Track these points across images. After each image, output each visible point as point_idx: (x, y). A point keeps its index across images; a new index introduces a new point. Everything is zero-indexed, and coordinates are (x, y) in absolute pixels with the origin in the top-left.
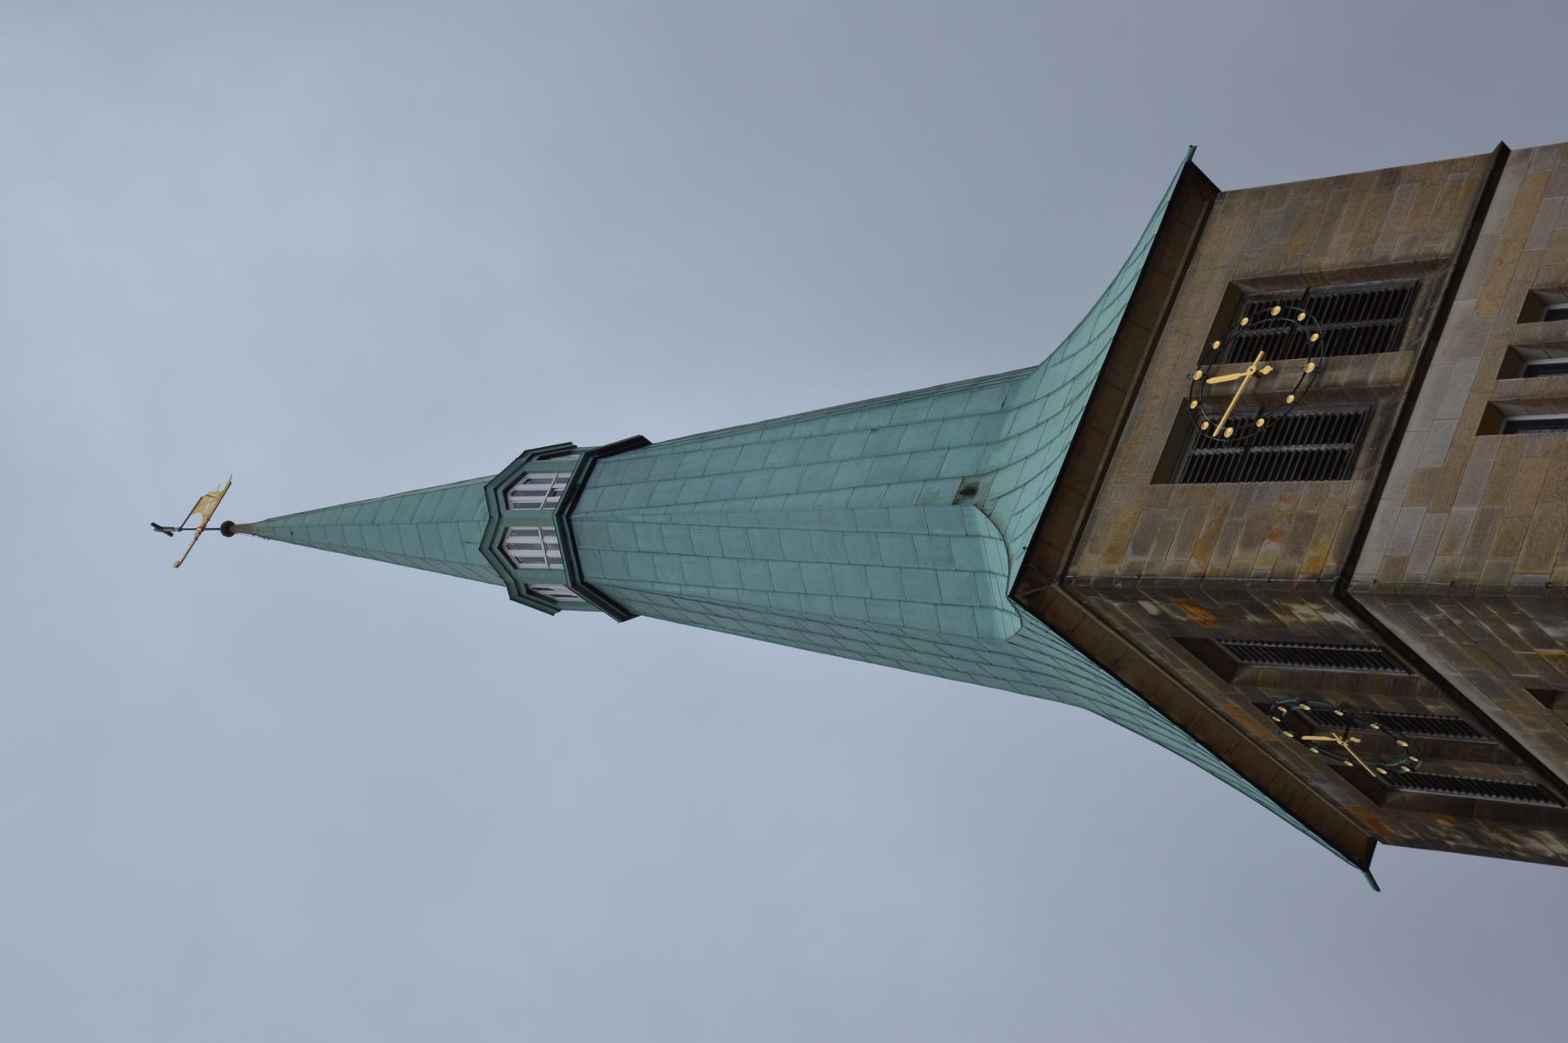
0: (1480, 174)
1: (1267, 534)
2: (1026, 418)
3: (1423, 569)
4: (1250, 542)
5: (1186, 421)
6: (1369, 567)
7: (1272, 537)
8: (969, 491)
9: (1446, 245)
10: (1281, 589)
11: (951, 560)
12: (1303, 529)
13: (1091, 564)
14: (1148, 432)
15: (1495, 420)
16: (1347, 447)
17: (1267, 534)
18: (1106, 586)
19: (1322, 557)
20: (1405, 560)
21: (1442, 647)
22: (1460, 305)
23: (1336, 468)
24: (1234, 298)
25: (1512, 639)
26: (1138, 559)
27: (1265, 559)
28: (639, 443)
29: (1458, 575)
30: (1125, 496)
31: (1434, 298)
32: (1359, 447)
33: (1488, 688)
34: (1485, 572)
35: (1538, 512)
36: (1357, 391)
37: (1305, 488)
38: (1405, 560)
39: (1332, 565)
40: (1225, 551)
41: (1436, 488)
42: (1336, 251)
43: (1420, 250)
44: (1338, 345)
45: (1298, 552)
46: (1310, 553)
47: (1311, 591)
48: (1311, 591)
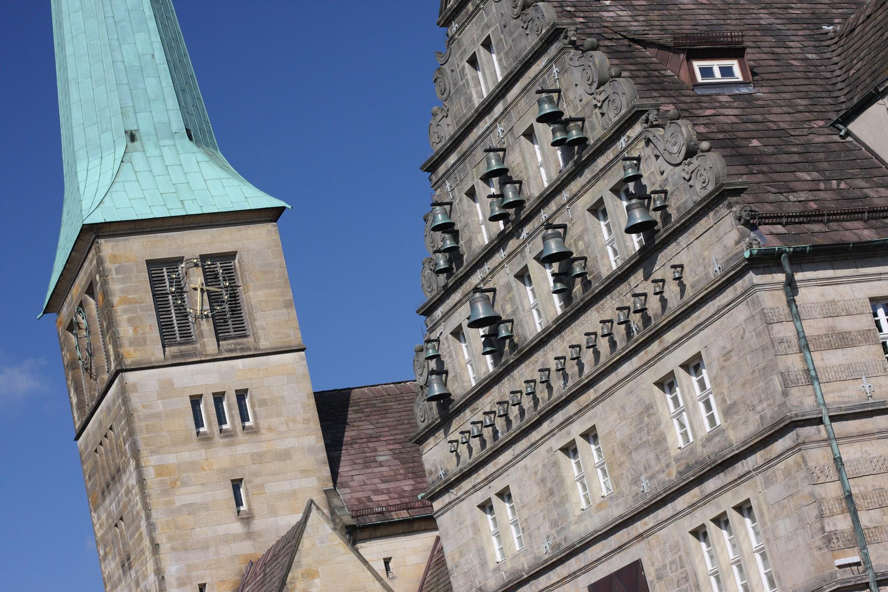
2: (168, 153)
3: (135, 400)
4: (130, 321)
5: (173, 263)
6: (130, 377)
7: (135, 329)
8: (132, 137)
9: (265, 344)
10: (117, 344)
11: (103, 132)
15: (195, 401)
16: (178, 339)
18: (100, 261)
19: (131, 355)
20: (137, 391)
26: (114, 272)
27: (125, 331)
29: (135, 415)
31: (242, 349)
32: (180, 344)
33: (109, 409)
34: (139, 424)
35: (164, 434)
36: (201, 334)
38: (137, 391)
40: (125, 311)
41: (167, 390)
43: (261, 333)
45: (131, 344)
46: (131, 350)
47: (119, 357)
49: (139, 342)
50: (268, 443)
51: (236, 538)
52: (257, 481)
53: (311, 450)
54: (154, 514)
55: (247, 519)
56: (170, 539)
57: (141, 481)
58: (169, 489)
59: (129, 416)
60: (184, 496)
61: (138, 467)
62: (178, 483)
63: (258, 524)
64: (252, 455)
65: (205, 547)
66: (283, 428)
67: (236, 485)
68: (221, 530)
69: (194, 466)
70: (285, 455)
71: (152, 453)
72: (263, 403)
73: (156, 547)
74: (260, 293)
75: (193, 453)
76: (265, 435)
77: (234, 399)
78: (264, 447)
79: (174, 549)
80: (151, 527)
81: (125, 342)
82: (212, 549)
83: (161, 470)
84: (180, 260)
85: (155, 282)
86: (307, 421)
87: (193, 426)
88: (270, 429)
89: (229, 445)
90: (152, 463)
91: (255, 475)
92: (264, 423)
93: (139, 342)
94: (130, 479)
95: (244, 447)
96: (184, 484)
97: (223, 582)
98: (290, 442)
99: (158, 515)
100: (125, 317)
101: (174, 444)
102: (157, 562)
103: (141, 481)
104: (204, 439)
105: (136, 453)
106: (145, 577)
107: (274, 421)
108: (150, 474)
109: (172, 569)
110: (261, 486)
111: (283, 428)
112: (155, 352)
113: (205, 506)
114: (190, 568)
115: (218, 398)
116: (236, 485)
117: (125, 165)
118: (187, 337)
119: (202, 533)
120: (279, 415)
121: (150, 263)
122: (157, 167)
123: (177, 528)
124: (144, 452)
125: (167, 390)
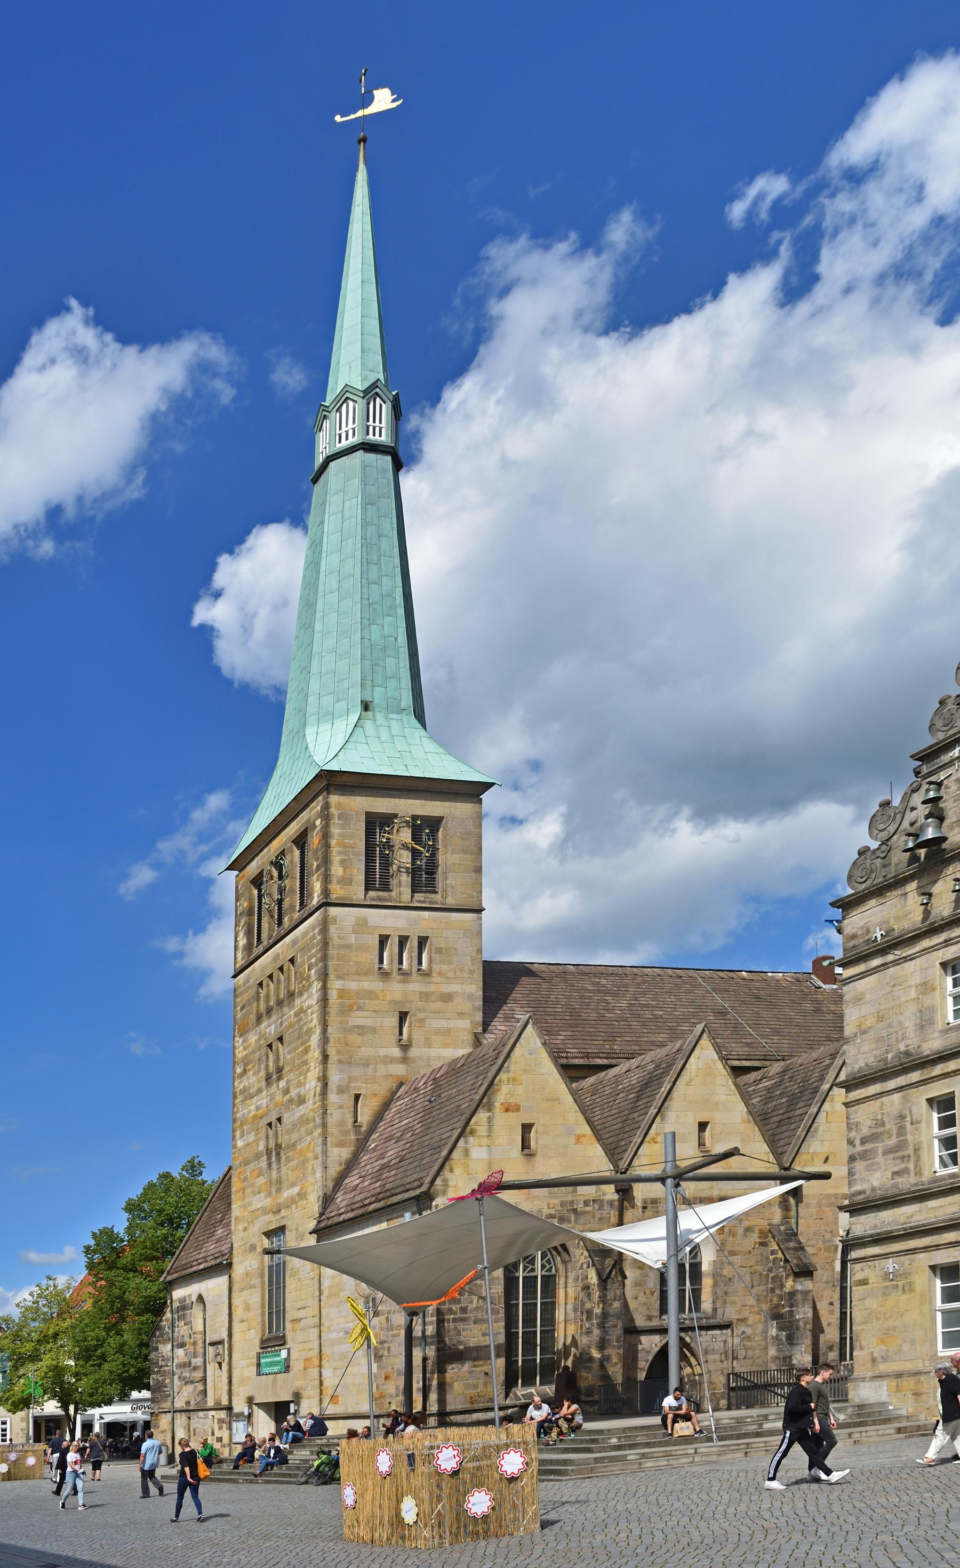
1: (347, 866)
3: (332, 929)
4: (342, 862)
6: (333, 911)
7: (344, 870)
9: (451, 901)
10: (326, 879)
14: (382, 805)
18: (326, 806)
20: (336, 923)
22: (426, 914)
23: (369, 886)
27: (337, 870)
30: (361, 804)
31: (430, 902)
34: (332, 952)
36: (400, 884)
38: (336, 923)
39: (334, 897)
40: (340, 853)
41: (361, 925)
44: (414, 872)
45: (339, 882)
46: (339, 887)
48: (326, 892)
49: (346, 881)
50: (437, 986)
51: (393, 1060)
52: (421, 1015)
53: (471, 997)
54: (330, 1030)
55: (405, 1047)
56: (339, 1052)
57: (324, 1000)
58: (345, 1011)
59: (325, 944)
60: (358, 1019)
61: (324, 989)
62: (355, 1007)
63: (413, 1052)
64: (421, 993)
65: (366, 1065)
66: (451, 975)
67: (403, 1016)
68: (382, 1052)
69: (371, 995)
70: (447, 998)
71: (338, 978)
72: (439, 951)
73: (325, 1057)
74: (455, 856)
75: (372, 984)
76: (436, 978)
77: (416, 944)
78: (432, 988)
79: (340, 1061)
81: (334, 880)
82: (372, 1067)
83: (342, 993)
84: (396, 816)
85: (370, 833)
86: (472, 972)
87: (377, 961)
88: (440, 974)
89: (404, 982)
90: (337, 987)
91: (420, 1010)
92: (436, 968)
93: (346, 881)
95: (416, 986)
96: (360, 1009)
97: (375, 1095)
98: (455, 988)
100: (339, 858)
101: (358, 974)
102: (325, 1070)
104: (384, 975)
105: (324, 977)
107: (445, 968)
108: (333, 995)
109: (335, 1078)
110: (422, 1021)
111: (451, 975)
112: (358, 892)
113: (373, 1030)
114: (350, 1079)
115: (403, 941)
116: (403, 1016)
117: (359, 730)
118: (386, 887)
119: (366, 1052)
120: (450, 963)
123: (346, 1044)
124: (332, 976)
125: (361, 925)
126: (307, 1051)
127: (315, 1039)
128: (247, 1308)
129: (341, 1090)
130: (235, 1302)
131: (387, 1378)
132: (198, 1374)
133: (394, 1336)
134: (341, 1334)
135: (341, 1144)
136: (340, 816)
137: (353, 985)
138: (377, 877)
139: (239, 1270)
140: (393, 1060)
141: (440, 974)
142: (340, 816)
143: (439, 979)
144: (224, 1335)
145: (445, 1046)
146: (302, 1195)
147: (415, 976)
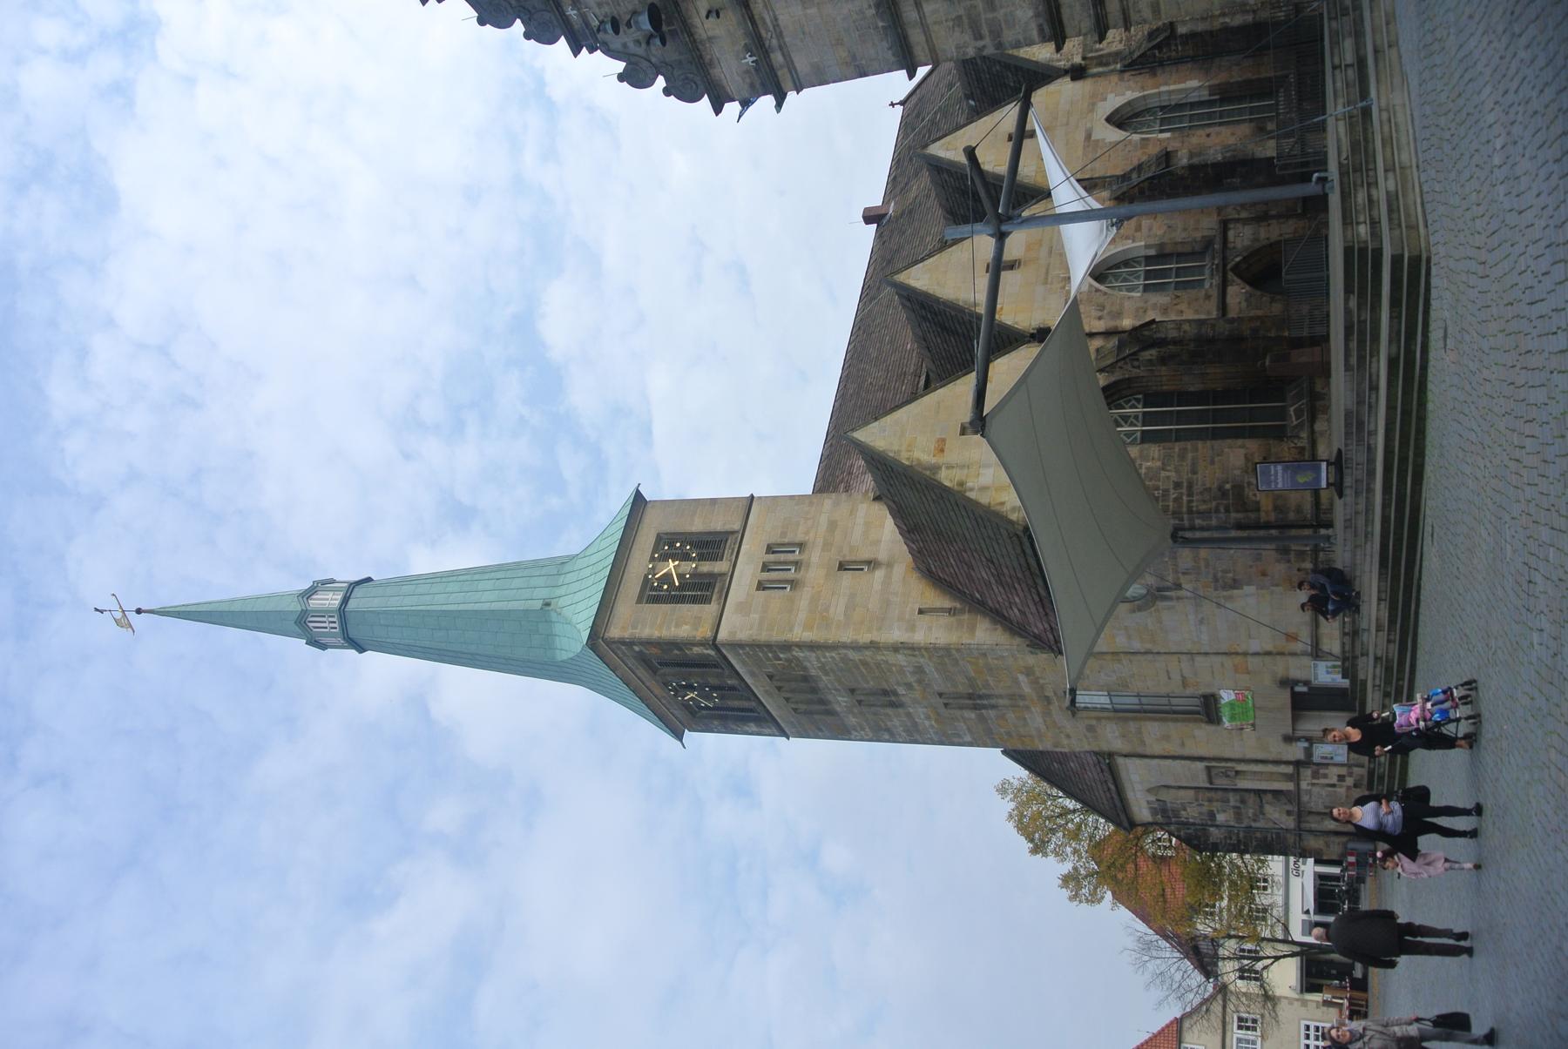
0: (746, 503)
2: (570, 577)
3: (743, 636)
4: (677, 626)
5: (646, 581)
10: (691, 643)
12: (697, 621)
13: (615, 632)
15: (761, 586)
17: (682, 624)
18: (622, 642)
21: (744, 663)
23: (705, 600)
24: (659, 538)
25: (768, 659)
28: (369, 580)
33: (753, 674)
34: (763, 637)
37: (696, 607)
39: (709, 634)
41: (744, 608)
42: (697, 525)
44: (701, 558)
47: (702, 644)
51: (888, 577)
55: (872, 564)
60: (838, 610)
61: (800, 646)
63: (882, 556)
68: (877, 586)
70: (833, 525)
71: (791, 630)
72: (784, 534)
75: (804, 599)
78: (820, 541)
80: (856, 647)
83: (808, 627)
85: (656, 600)
88: (807, 533)
89: (808, 565)
92: (799, 538)
93: (697, 621)
94: (812, 661)
95: (815, 556)
96: (827, 609)
98: (823, 520)
99: (847, 636)
103: (812, 646)
105: (787, 646)
106: (901, 671)
108: (808, 636)
109: (896, 635)
112: (711, 609)
116: (842, 567)
121: (639, 601)
122: (576, 587)
126: (865, 664)
127: (852, 654)
128: (1166, 738)
129: (912, 628)
130: (1157, 749)
131: (1264, 574)
132: (1251, 799)
133: (1207, 565)
134: (1204, 628)
135: (972, 629)
136: (634, 627)
137: (802, 616)
138: (701, 589)
139: (1118, 745)
140: (888, 577)
141: (807, 533)
142: (634, 627)
143: (812, 535)
144: (1201, 765)
145: (882, 526)
146: (1029, 672)
147: (804, 557)
